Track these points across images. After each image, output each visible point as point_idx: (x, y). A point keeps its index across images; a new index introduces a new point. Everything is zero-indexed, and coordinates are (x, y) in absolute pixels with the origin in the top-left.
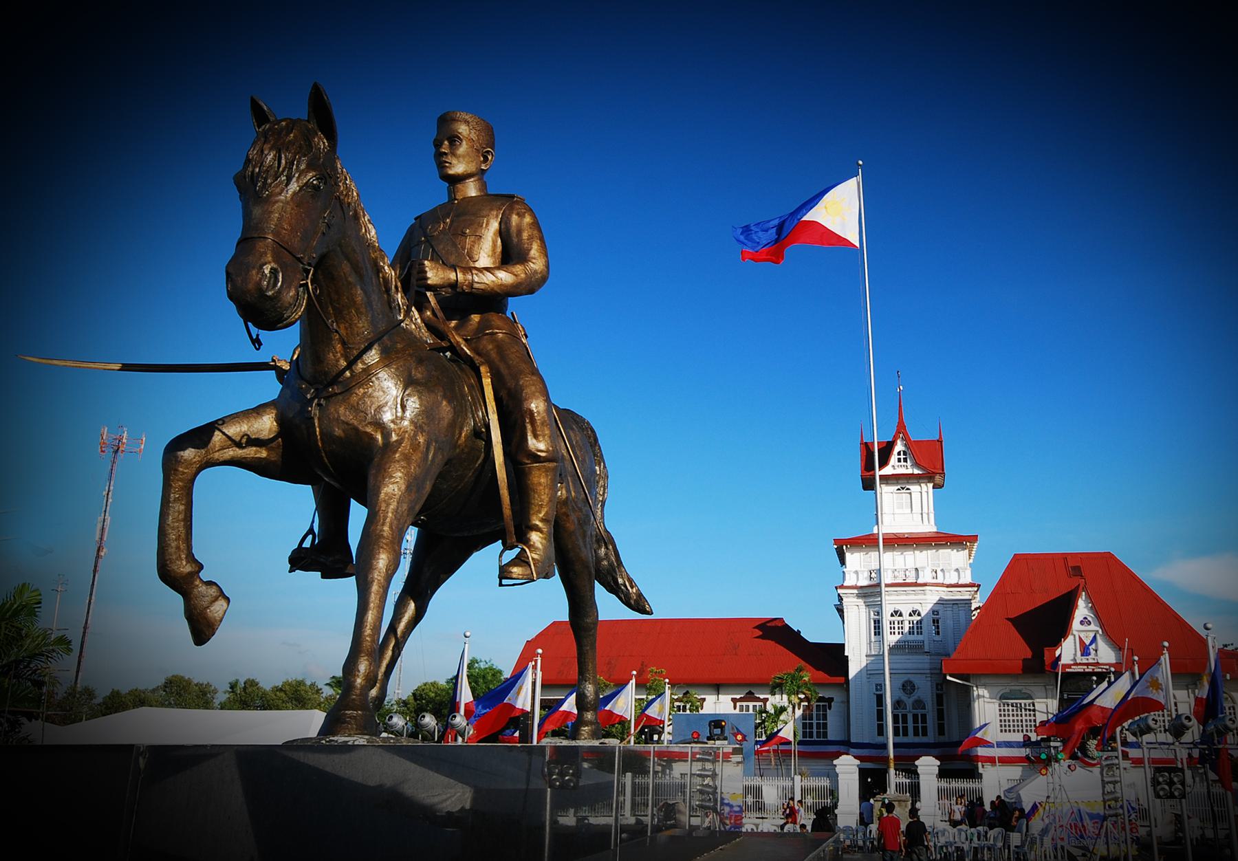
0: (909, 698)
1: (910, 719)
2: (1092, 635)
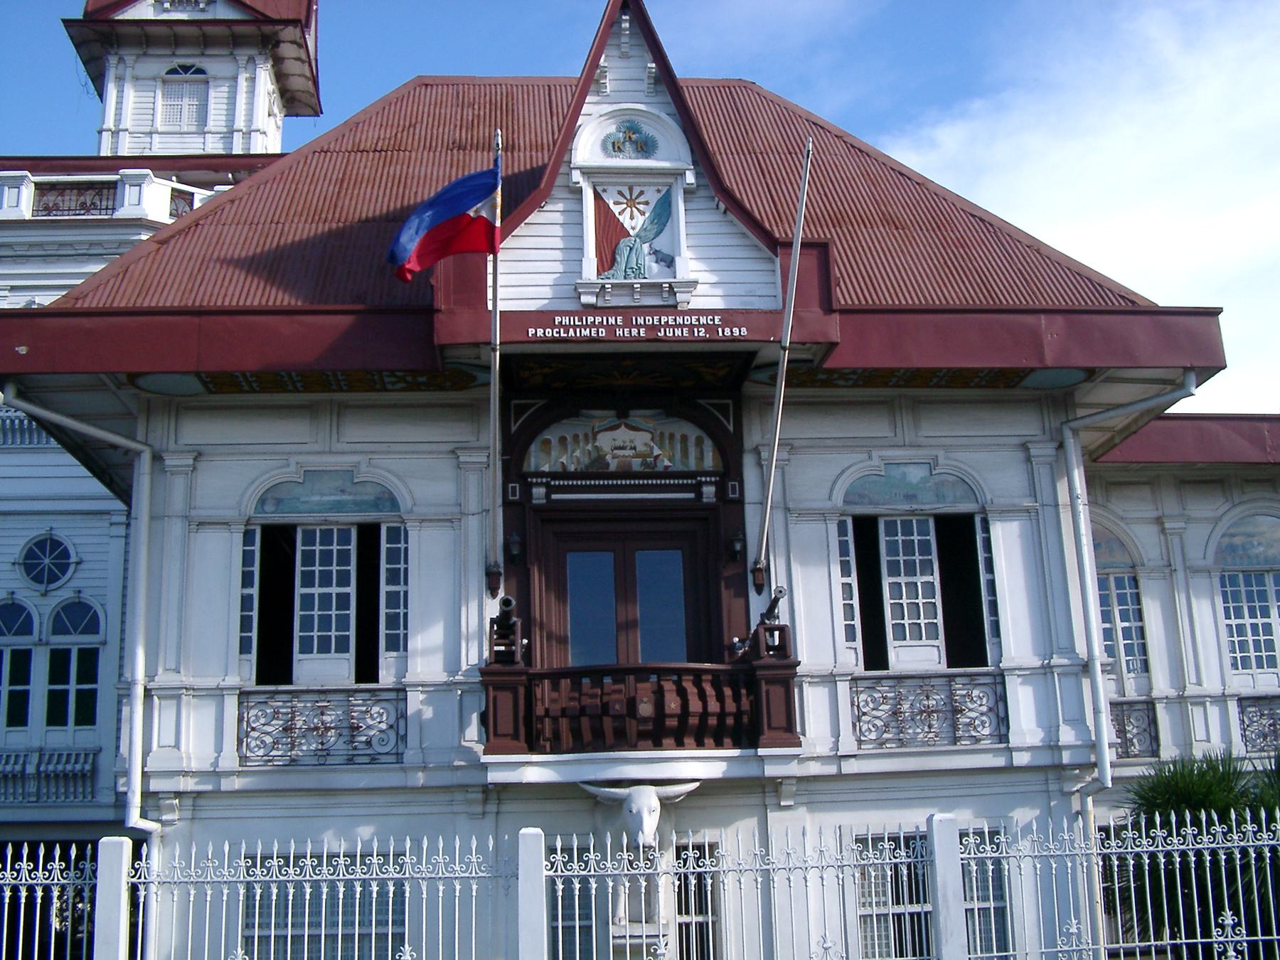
0: (45, 594)
1: (40, 667)
2: (652, 196)
